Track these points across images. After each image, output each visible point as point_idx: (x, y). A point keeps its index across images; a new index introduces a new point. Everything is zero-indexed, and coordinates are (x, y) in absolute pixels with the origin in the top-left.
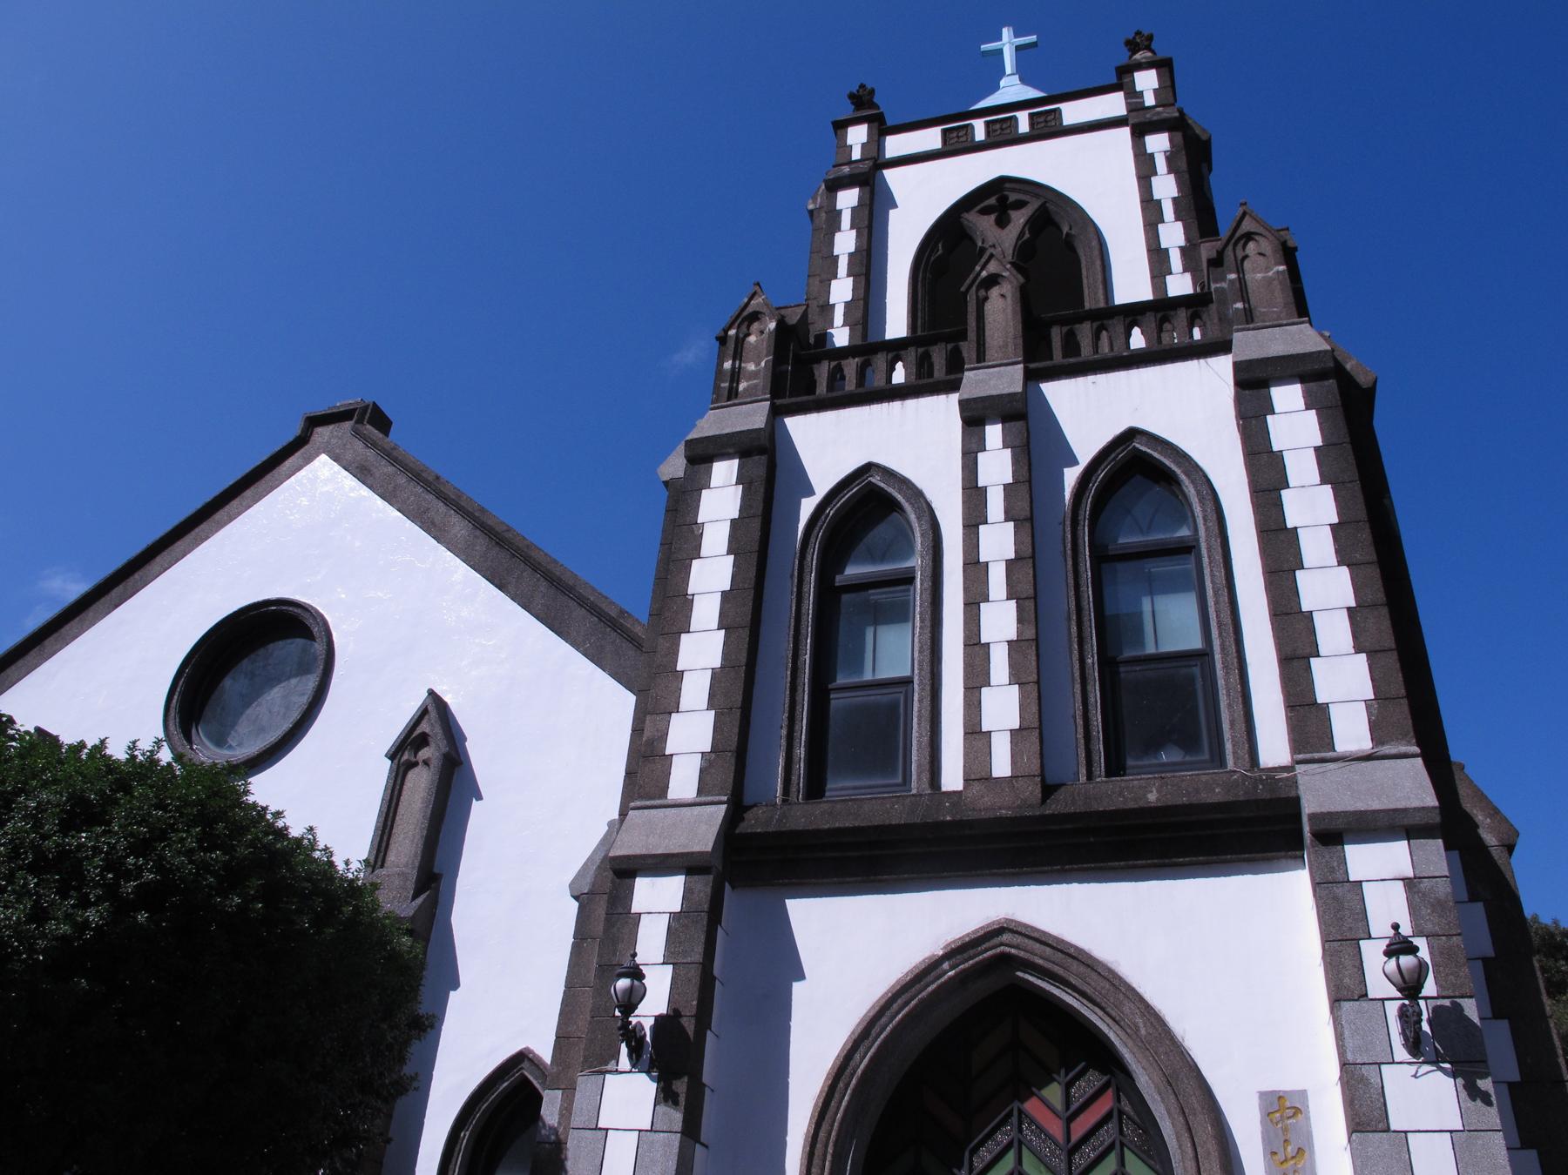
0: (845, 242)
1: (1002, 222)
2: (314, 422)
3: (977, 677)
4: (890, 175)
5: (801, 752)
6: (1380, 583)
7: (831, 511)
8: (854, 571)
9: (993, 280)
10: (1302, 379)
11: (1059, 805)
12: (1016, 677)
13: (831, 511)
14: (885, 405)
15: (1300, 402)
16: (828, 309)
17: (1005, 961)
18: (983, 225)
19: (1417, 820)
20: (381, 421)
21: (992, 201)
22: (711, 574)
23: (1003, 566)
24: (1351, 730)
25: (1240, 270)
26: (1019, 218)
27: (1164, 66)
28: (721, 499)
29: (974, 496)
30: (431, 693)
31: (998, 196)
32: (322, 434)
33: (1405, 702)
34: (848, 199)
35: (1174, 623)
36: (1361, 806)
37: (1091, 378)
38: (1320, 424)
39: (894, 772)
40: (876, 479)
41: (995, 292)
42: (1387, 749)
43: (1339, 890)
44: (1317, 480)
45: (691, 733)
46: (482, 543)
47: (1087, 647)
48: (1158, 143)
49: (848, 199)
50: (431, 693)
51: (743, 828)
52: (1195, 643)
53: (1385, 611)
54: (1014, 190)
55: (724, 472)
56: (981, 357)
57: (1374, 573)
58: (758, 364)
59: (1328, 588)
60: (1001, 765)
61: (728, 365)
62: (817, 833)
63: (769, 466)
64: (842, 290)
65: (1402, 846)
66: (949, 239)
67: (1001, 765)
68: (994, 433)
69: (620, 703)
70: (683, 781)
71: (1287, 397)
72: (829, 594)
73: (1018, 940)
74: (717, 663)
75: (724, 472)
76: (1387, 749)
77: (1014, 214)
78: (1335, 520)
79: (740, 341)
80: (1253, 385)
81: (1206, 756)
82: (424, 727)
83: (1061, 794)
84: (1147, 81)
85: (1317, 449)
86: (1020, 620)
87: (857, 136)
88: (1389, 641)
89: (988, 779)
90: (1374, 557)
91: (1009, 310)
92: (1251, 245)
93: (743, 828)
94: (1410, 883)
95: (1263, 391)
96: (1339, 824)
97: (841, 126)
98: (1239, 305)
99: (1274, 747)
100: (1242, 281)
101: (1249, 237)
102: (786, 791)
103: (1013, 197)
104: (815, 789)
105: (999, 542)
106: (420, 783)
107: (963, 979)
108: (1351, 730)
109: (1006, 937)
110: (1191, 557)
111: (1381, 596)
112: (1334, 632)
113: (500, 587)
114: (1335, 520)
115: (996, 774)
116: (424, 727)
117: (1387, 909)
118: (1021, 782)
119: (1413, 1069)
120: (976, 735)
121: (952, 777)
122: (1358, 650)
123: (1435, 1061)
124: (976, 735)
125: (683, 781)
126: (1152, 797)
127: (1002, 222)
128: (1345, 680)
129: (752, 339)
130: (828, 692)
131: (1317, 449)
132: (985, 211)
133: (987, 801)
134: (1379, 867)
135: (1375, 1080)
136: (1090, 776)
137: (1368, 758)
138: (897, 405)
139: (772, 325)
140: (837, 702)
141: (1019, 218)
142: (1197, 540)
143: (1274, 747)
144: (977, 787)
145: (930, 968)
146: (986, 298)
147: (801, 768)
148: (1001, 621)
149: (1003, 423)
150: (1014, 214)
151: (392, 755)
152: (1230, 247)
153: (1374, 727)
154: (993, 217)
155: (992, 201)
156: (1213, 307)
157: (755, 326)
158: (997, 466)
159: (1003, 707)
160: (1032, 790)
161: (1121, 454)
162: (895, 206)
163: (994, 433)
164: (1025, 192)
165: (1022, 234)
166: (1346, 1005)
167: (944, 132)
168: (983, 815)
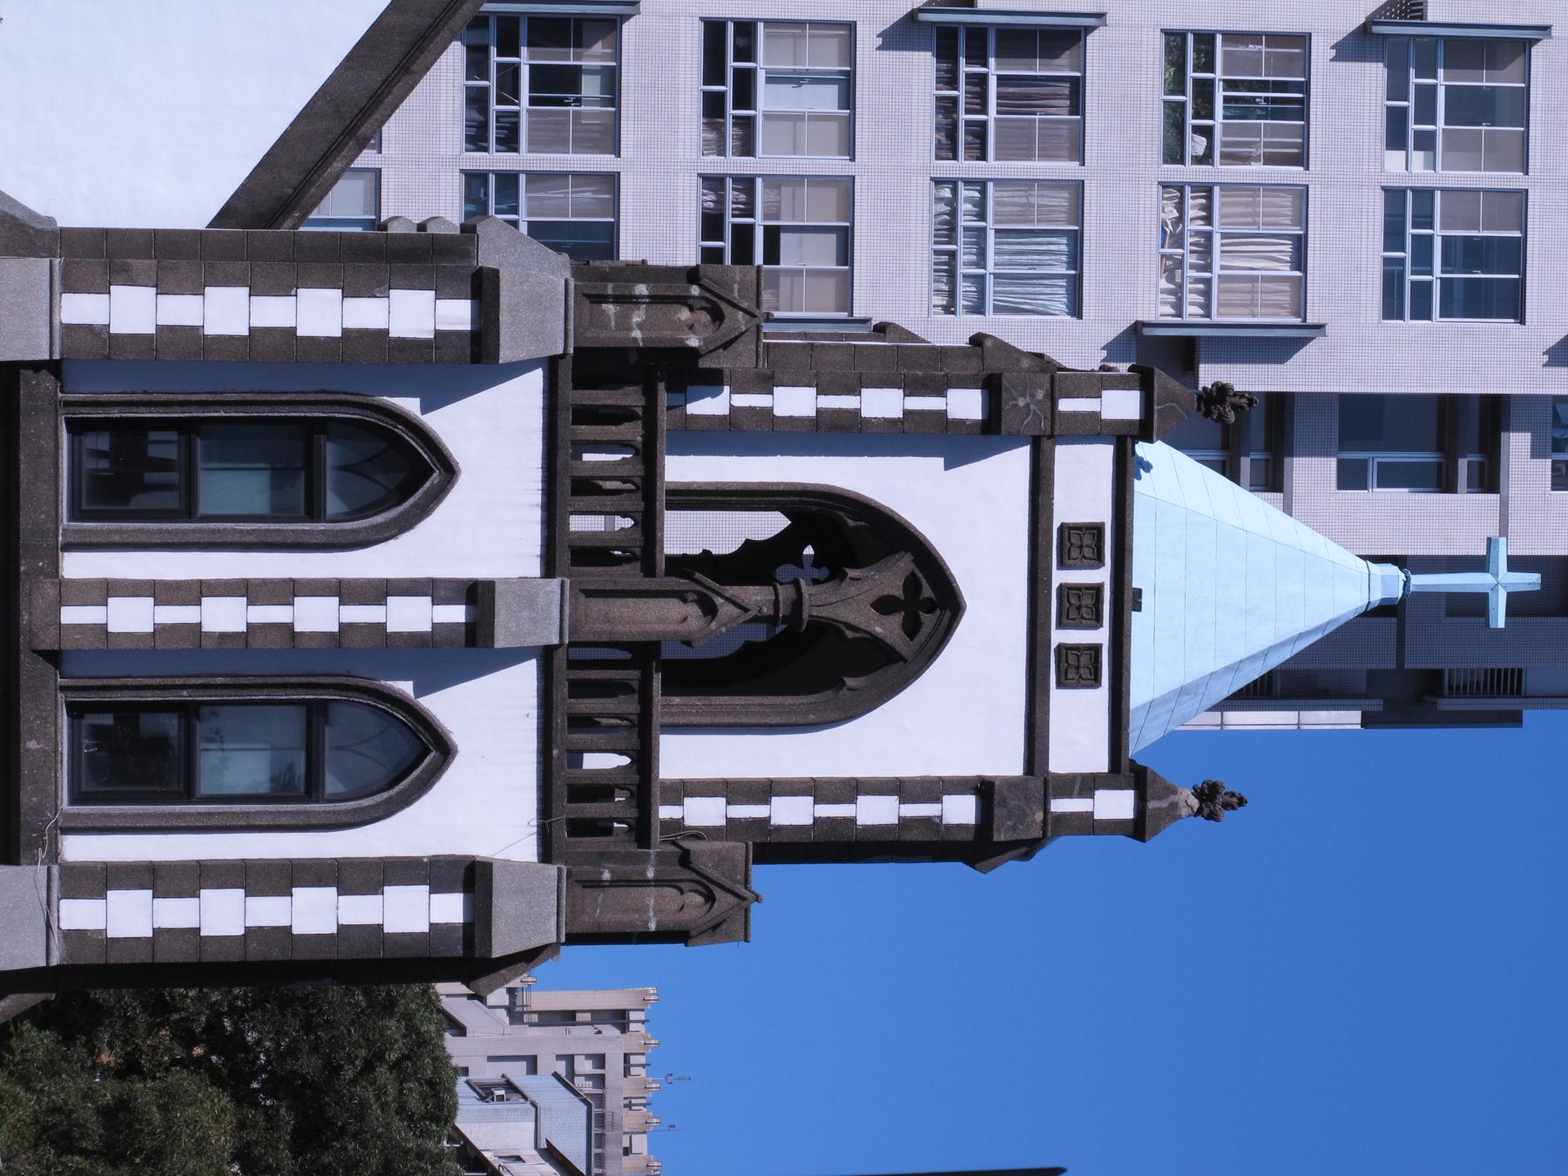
3: (163, 592)
4: (1020, 458)
5: (115, 413)
6: (222, 959)
8: (331, 453)
9: (710, 610)
10: (468, 927)
11: (29, 666)
12: (160, 630)
13: (400, 430)
14: (539, 485)
15: (439, 918)
16: (766, 384)
18: (890, 578)
21: (927, 592)
22: (319, 313)
23: (287, 620)
24: (78, 914)
25: (658, 882)
26: (888, 628)
27: (1137, 828)
28: (418, 313)
29: (379, 591)
31: (932, 602)
33: (102, 961)
34: (966, 404)
35: (236, 766)
37: (534, 713)
38: (410, 934)
39: (77, 514)
40: (435, 477)
41: (693, 610)
42: (56, 941)
44: (344, 921)
45: (132, 310)
47: (201, 692)
48: (960, 810)
49: (966, 404)
51: (26, 374)
52: (205, 786)
53: (193, 959)
54: (939, 621)
55: (457, 314)
56: (590, 594)
57: (235, 956)
58: (640, 326)
59: (223, 915)
60: (71, 615)
61: (642, 289)
63: (473, 360)
67: (71, 615)
68: (456, 614)
69: (191, 200)
70: (80, 309)
71: (450, 908)
75: (457, 314)
76: (56, 941)
77: (895, 620)
78: (295, 931)
79: (683, 301)
80: (472, 877)
81: (84, 788)
83: (43, 665)
84: (1116, 804)
85: (380, 927)
86: (223, 636)
88: (163, 957)
89: (61, 602)
90: (250, 958)
91: (648, 628)
92: (699, 899)
93: (26, 374)
95: (460, 885)
98: (606, 876)
99: (79, 849)
100: (645, 883)
101: (710, 898)
102: (68, 404)
103: (928, 620)
105: (316, 616)
108: (78, 914)
110: (298, 793)
112: (176, 913)
114: (295, 931)
115: (64, 610)
118: (53, 631)
120: (106, 590)
121: (76, 566)
122: (156, 931)
124: (106, 590)
125: (80, 309)
126: (32, 745)
127: (884, 605)
128: (129, 916)
129: (685, 314)
131: (380, 927)
132: (912, 584)
133: (39, 602)
136: (63, 689)
137: (48, 926)
138: (537, 498)
139: (693, 342)
142: (317, 802)
143: (79, 849)
144: (50, 591)
146: (685, 601)
148: (224, 617)
149: (466, 624)
150: (895, 620)
152: (694, 876)
153: (80, 935)
154: (898, 592)
155: (927, 592)
156: (633, 848)
157: (704, 317)
158: (410, 616)
159: (131, 617)
160: (47, 642)
162: (948, 466)
163: (456, 614)
167: (1097, 529)
168: (23, 599)
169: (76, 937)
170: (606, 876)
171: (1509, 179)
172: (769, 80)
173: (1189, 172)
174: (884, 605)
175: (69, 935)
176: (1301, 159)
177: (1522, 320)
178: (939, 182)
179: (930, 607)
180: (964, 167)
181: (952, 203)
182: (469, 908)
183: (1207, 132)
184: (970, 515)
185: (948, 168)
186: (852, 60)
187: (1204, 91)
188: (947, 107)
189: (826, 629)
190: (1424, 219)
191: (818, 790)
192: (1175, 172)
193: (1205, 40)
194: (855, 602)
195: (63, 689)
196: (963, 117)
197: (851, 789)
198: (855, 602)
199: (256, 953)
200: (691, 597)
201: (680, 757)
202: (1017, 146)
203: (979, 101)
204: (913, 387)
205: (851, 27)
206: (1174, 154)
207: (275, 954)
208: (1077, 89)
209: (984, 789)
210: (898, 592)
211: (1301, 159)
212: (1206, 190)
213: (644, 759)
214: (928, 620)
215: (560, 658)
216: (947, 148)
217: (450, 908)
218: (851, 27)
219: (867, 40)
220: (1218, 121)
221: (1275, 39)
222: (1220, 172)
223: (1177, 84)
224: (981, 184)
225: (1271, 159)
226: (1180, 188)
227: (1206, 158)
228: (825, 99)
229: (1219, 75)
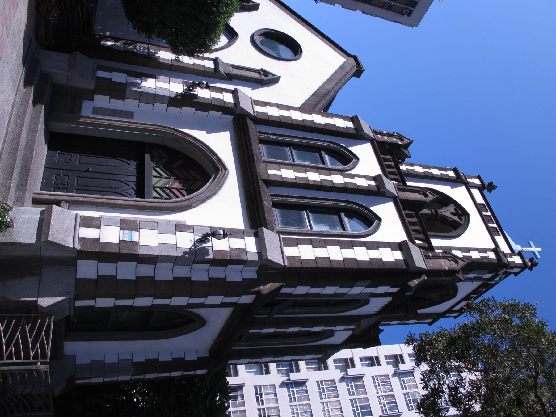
0: (436, 172)
1: (452, 213)
2: (355, 58)
7: (343, 149)
10: (405, 260)
12: (297, 178)
13: (343, 149)
17: (218, 170)
18: (451, 208)
19: (264, 253)
20: (358, 73)
21: (460, 212)
30: (280, 77)
32: (352, 60)
34: (451, 174)
36: (266, 241)
37: (397, 214)
40: (354, 160)
43: (241, 233)
46: (325, 91)
49: (451, 174)
50: (280, 77)
54: (465, 218)
60: (270, 172)
62: (248, 132)
64: (419, 169)
65: (255, 250)
66: (446, 200)
72: (318, 149)
73: (223, 173)
82: (270, 76)
87: (477, 181)
92: (454, 263)
94: (245, 250)
96: (260, 235)
97: (479, 177)
101: (457, 262)
103: (463, 218)
104: (262, 141)
106: (256, 75)
107: (212, 162)
109: (224, 170)
111: (334, 266)
113: (313, 95)
116: (270, 76)
117: (237, 243)
119: (193, 240)
123: (195, 245)
127: (452, 213)
129: (395, 139)
130: (290, 147)
134: (249, 244)
135: (189, 231)
136: (271, 195)
140: (288, 149)
141: (456, 218)
145: (214, 154)
146: (420, 194)
147: (267, 136)
151: (262, 70)
155: (460, 212)
160: (265, 177)
161: (372, 216)
164: (465, 221)
165: (450, 218)
166: (209, 229)
169: (290, 258)
170: (430, 255)
171: (365, 396)
172: (265, 394)
173: (324, 400)
175: (288, 257)
176: (338, 397)
177: (372, 415)
178: (291, 406)
180: (293, 403)
181: (293, 409)
182: (403, 255)
183: (325, 395)
185: (291, 404)
186: (275, 390)
187: (323, 389)
188: (290, 395)
189: (444, 218)
190: (356, 403)
192: (322, 401)
193: (321, 381)
195: (271, 195)
196: (292, 396)
198: (447, 212)
199: (348, 266)
200: (421, 193)
202: (300, 399)
203: (294, 394)
204: (440, 169)
205: (274, 385)
206: (321, 398)
207: (354, 266)
208: (307, 391)
211: (338, 397)
212: (326, 403)
214: (463, 218)
216: (291, 401)
217: (398, 255)
218: (274, 385)
219: (277, 387)
220: (326, 393)
221: (331, 381)
222: (328, 400)
223: (319, 389)
224: (296, 406)
225: (334, 397)
226: (323, 403)
227: (326, 398)
228: (272, 396)
229: (324, 386)
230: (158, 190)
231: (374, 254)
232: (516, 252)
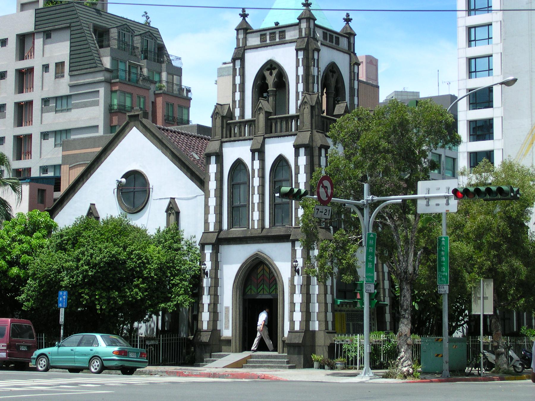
12: (258, 210)
18: (267, 73)
21: (269, 66)
26: (275, 72)
31: (271, 66)
48: (301, 55)
60: (256, 227)
66: (260, 78)
67: (256, 227)
74: (215, 205)
75: (213, 159)
82: (171, 206)
103: (274, 66)
106: (172, 217)
127: (271, 74)
132: (268, 70)
141: (275, 72)
151: (167, 211)
154: (269, 72)
160: (260, 230)
165: (274, 79)
174: (271, 74)
179: (271, 65)
184: (255, 61)
191: (297, 83)
194: (271, 80)
197: (297, 76)
198: (271, 80)
201: (292, 111)
209: (297, 50)
210: (269, 72)
213: (292, 117)
214: (274, 66)
215: (266, 136)
230: (271, 290)
231: (302, 170)
232: (298, 21)
